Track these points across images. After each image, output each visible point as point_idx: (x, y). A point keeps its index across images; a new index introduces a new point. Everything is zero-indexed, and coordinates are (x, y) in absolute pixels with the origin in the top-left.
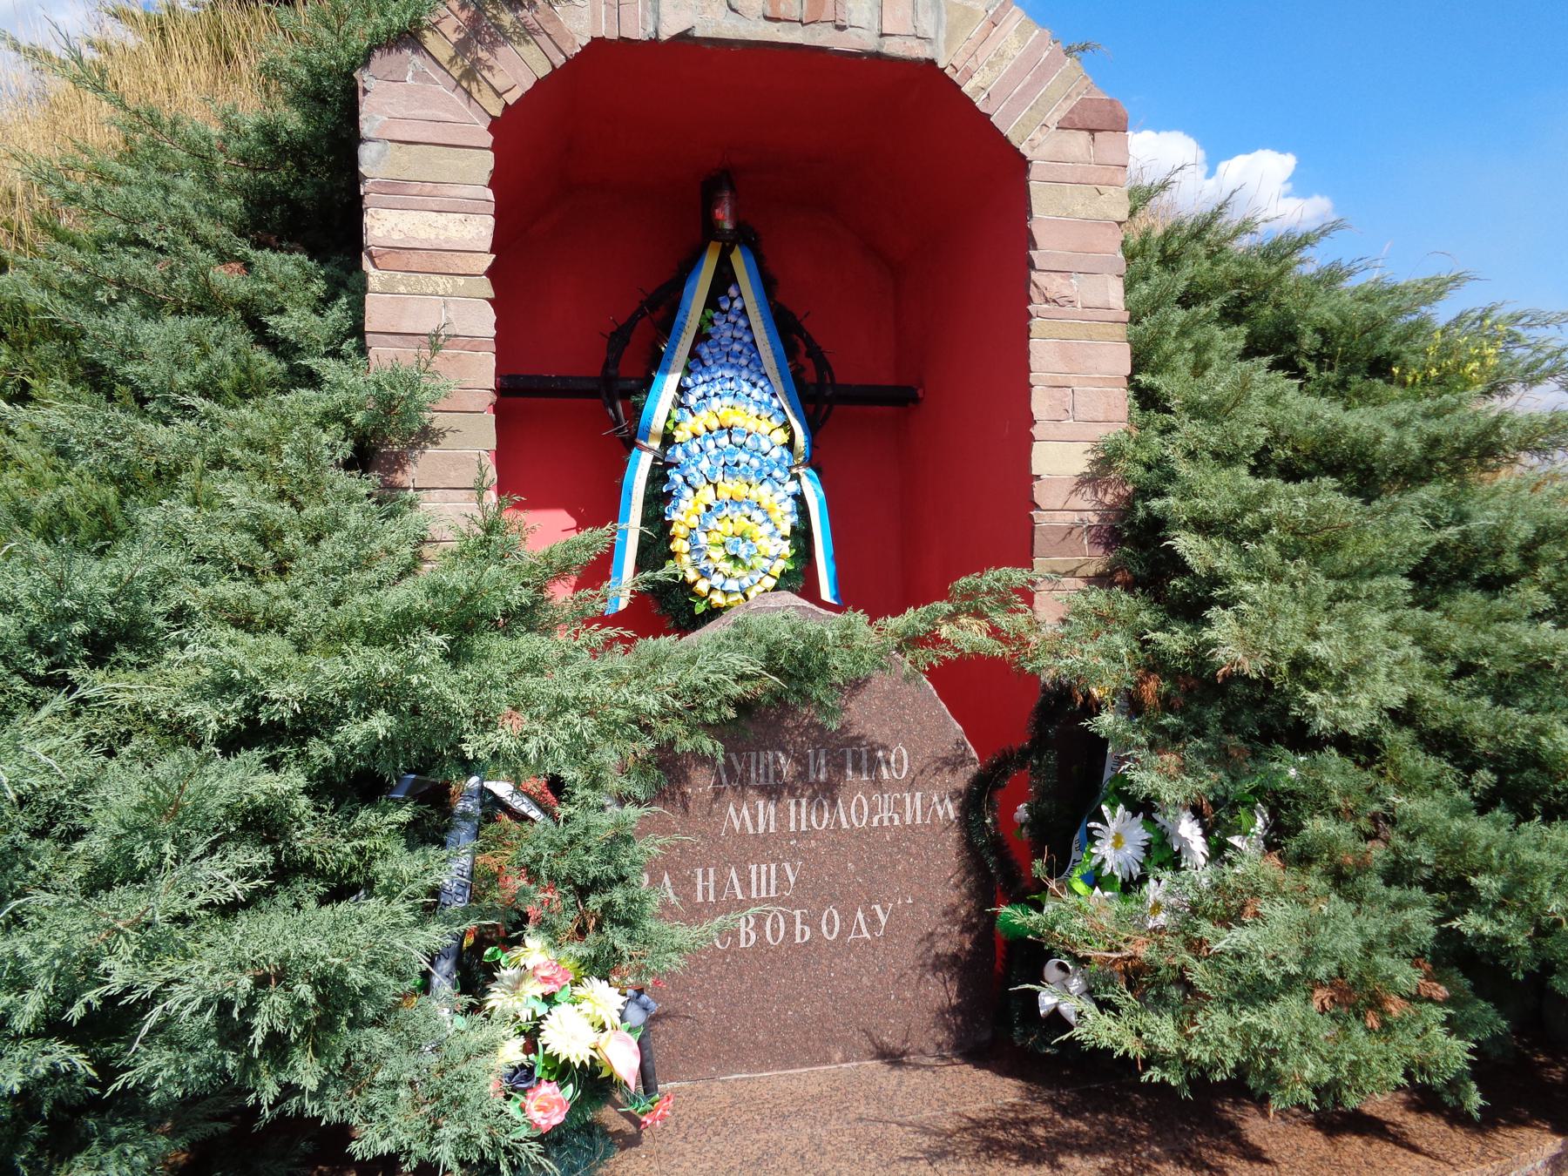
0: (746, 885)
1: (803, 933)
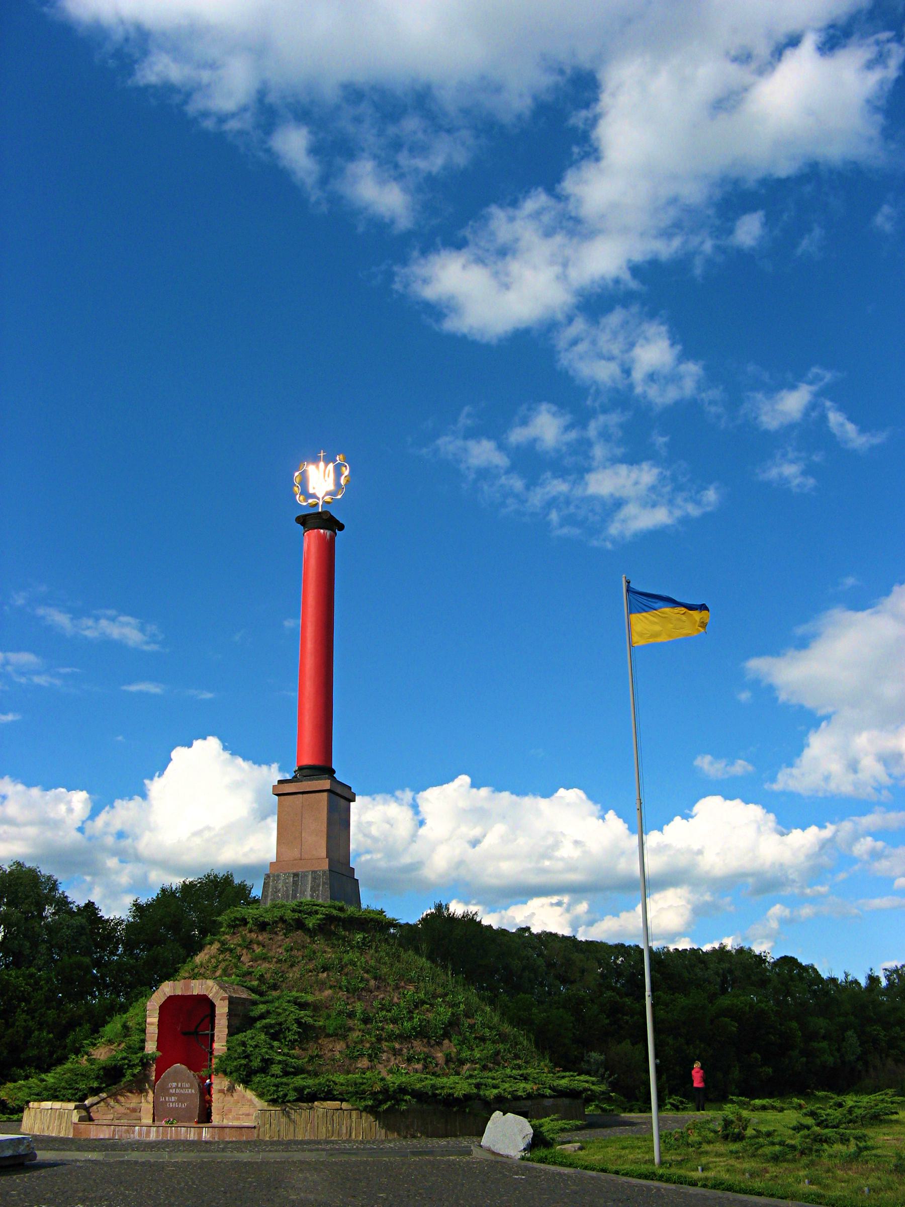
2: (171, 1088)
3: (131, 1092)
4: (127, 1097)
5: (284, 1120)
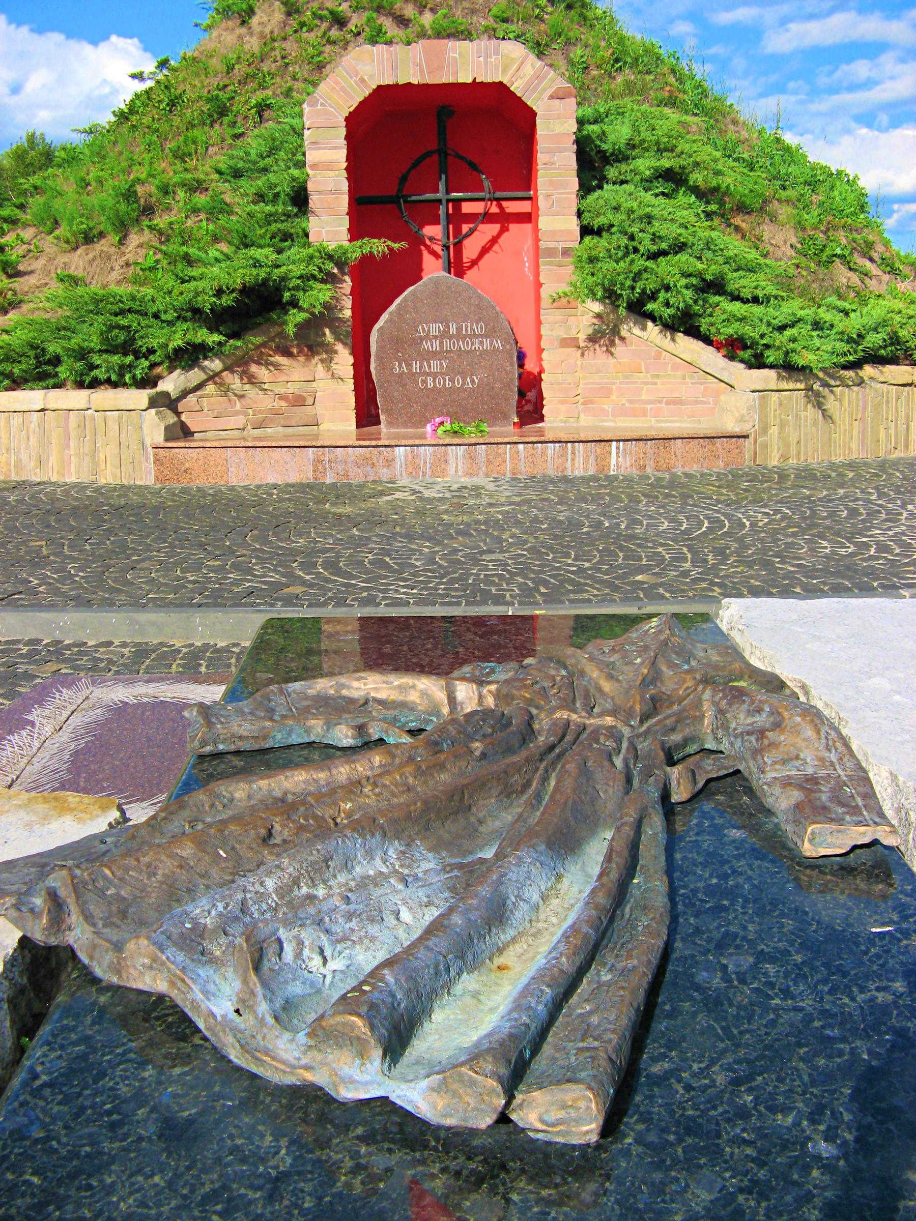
0: (430, 367)
1: (449, 384)
2: (427, 337)
3: (287, 353)
4: (277, 366)
5: (811, 412)
